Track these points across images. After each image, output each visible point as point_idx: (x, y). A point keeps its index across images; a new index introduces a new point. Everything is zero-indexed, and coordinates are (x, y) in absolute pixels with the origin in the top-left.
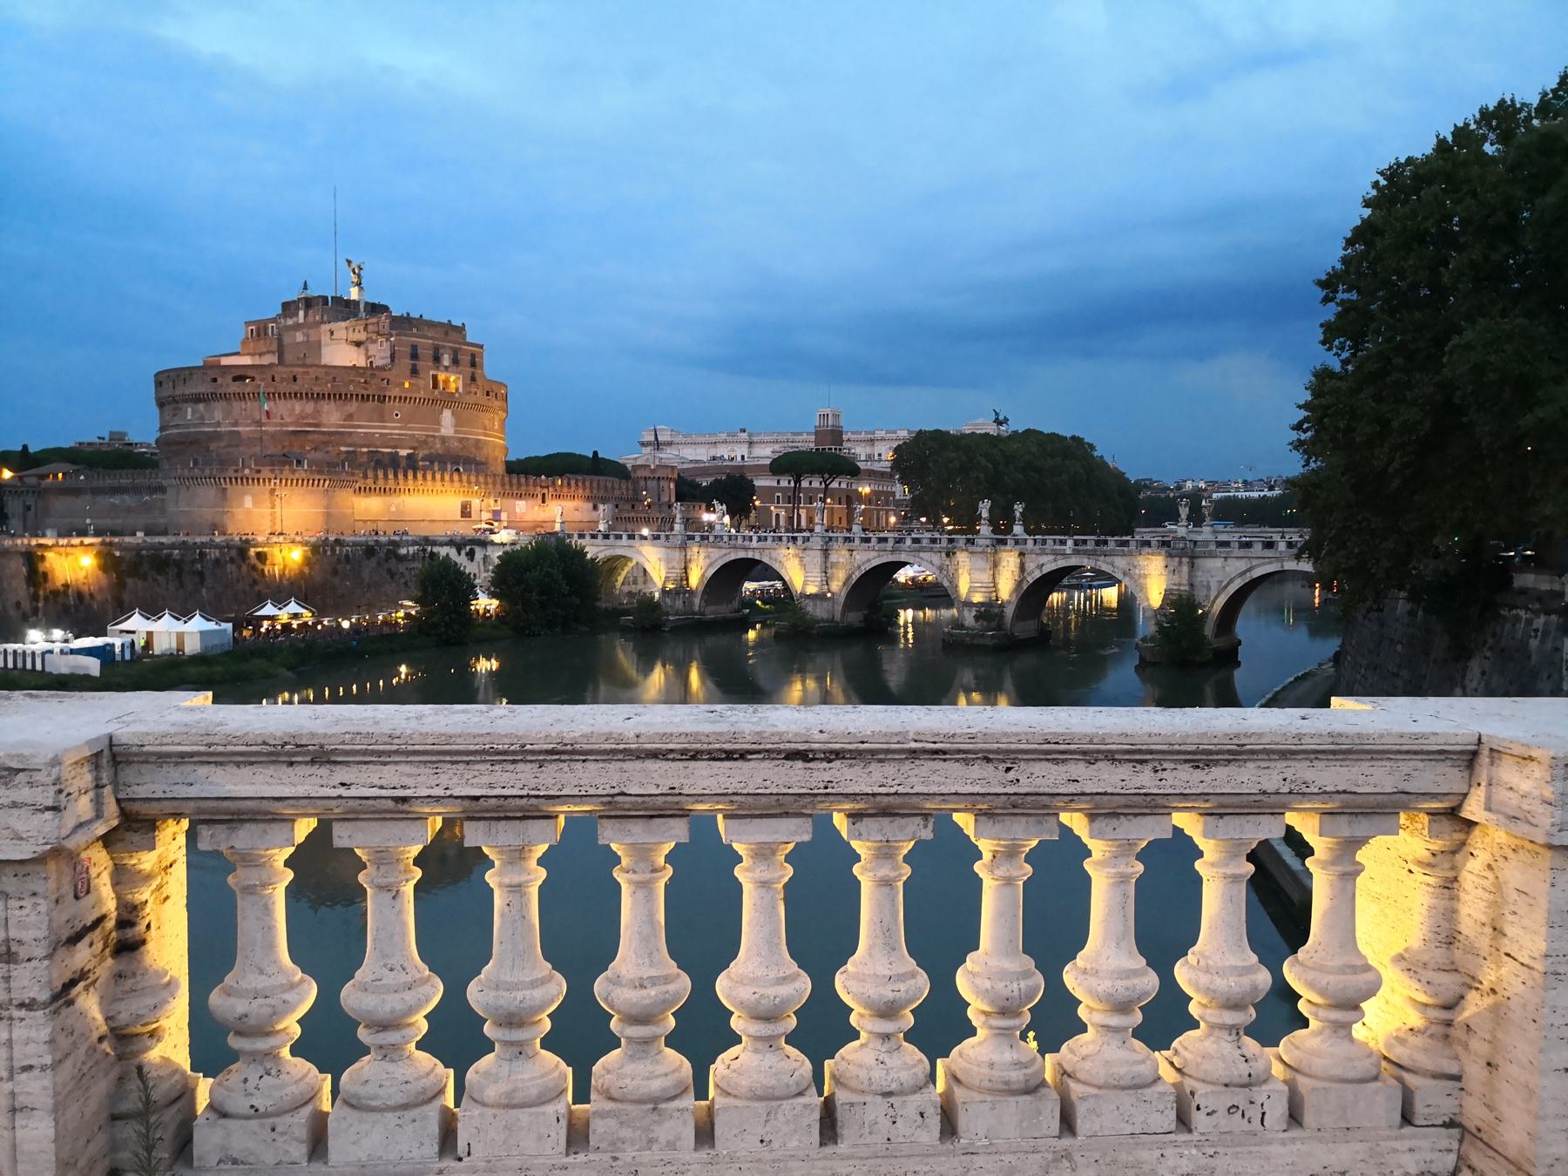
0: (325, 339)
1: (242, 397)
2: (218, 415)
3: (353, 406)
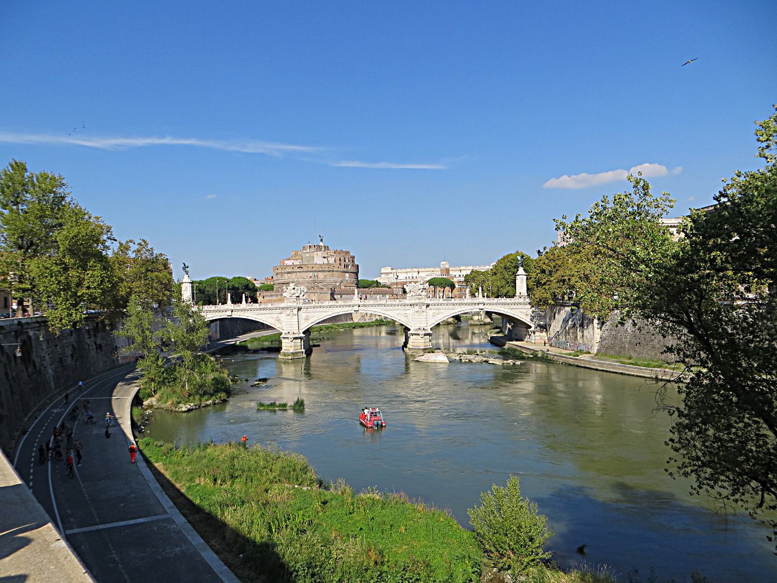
0: (315, 256)
1: (300, 272)
2: (294, 277)
3: (326, 273)
